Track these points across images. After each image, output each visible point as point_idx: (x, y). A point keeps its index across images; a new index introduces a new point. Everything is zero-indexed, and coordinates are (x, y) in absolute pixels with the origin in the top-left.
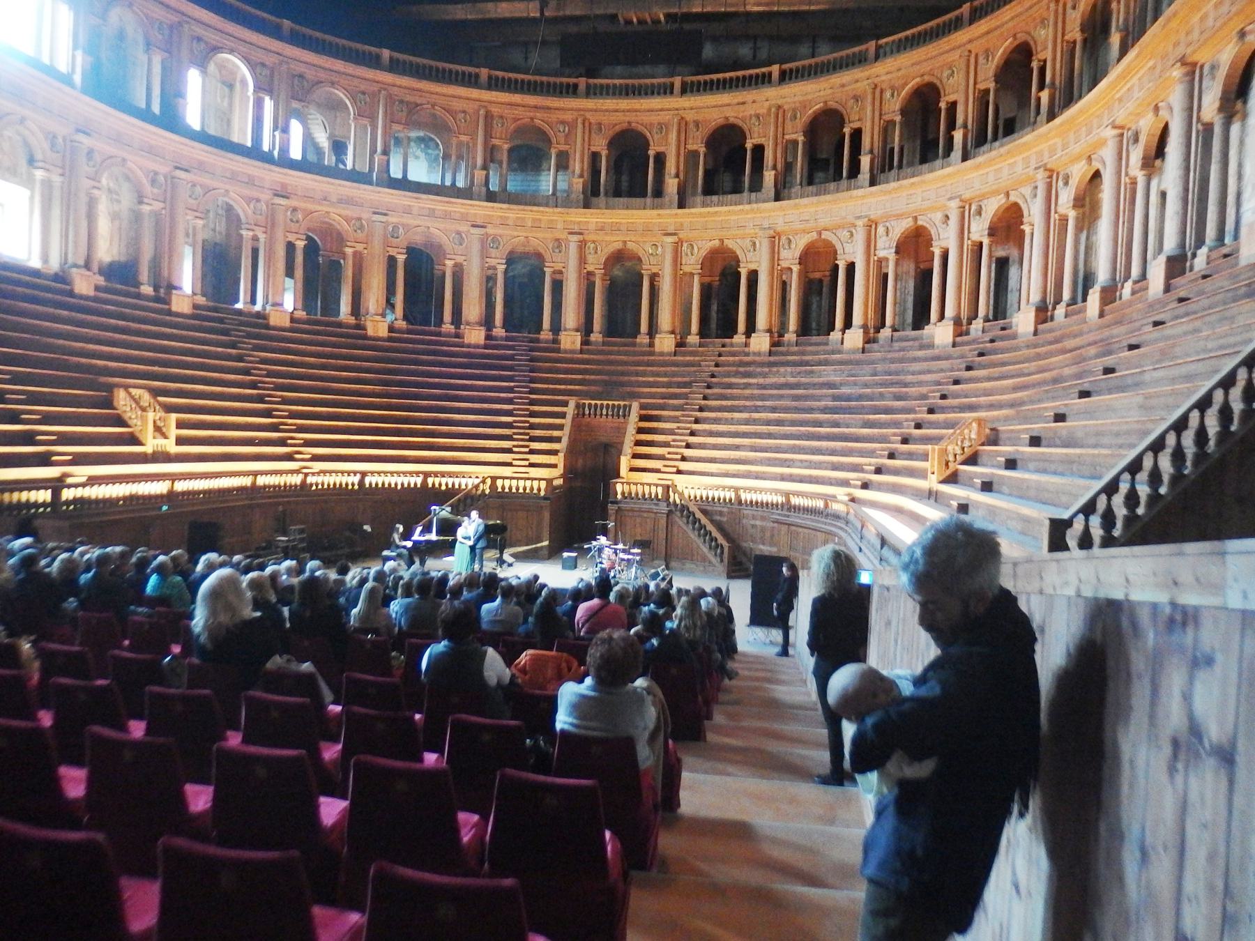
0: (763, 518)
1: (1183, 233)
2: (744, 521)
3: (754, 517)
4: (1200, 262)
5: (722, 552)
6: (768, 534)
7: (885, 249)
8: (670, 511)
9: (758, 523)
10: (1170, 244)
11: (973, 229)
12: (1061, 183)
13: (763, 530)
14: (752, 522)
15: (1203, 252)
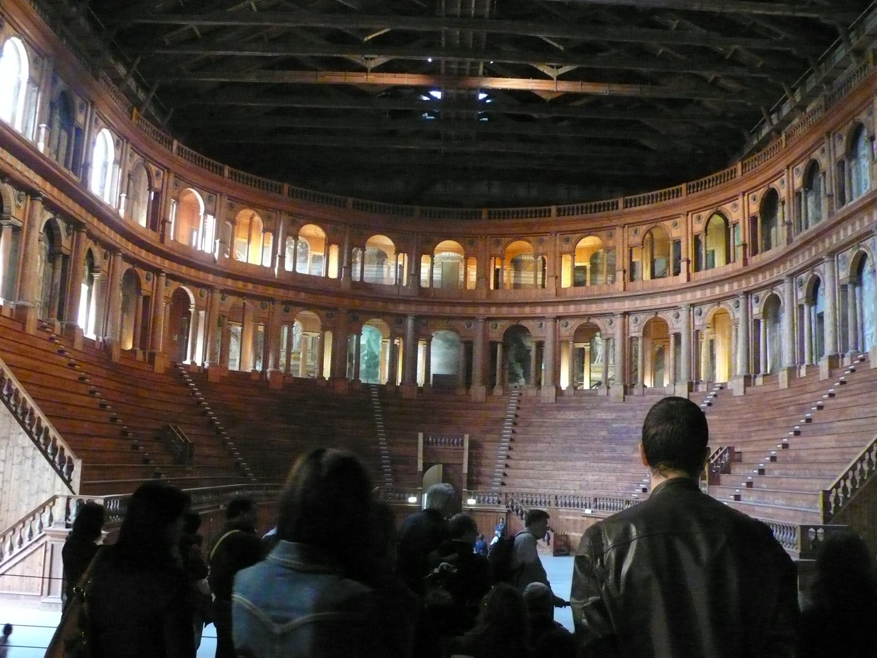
0: (575, 514)
1: (835, 343)
2: (560, 517)
3: (568, 514)
4: (847, 361)
5: (549, 538)
6: (579, 525)
7: (635, 330)
8: (509, 511)
9: (571, 517)
10: (829, 349)
11: (697, 323)
12: (754, 301)
13: (575, 522)
14: (567, 517)
15: (848, 354)
